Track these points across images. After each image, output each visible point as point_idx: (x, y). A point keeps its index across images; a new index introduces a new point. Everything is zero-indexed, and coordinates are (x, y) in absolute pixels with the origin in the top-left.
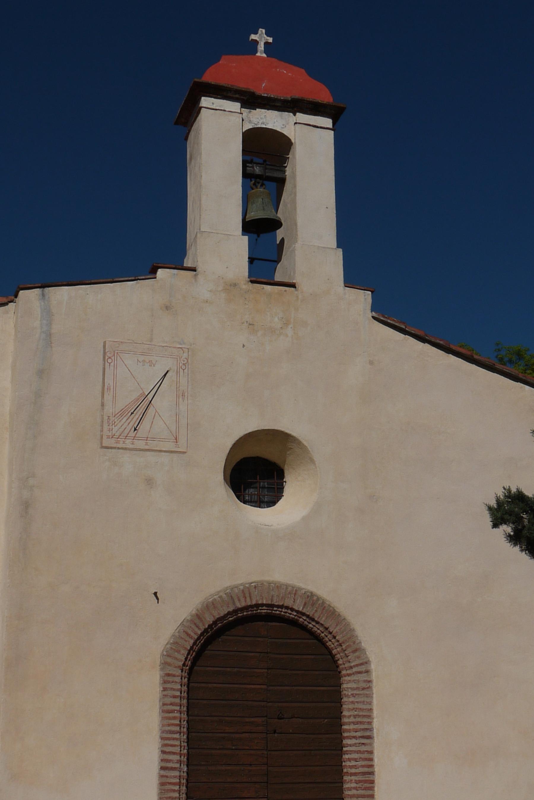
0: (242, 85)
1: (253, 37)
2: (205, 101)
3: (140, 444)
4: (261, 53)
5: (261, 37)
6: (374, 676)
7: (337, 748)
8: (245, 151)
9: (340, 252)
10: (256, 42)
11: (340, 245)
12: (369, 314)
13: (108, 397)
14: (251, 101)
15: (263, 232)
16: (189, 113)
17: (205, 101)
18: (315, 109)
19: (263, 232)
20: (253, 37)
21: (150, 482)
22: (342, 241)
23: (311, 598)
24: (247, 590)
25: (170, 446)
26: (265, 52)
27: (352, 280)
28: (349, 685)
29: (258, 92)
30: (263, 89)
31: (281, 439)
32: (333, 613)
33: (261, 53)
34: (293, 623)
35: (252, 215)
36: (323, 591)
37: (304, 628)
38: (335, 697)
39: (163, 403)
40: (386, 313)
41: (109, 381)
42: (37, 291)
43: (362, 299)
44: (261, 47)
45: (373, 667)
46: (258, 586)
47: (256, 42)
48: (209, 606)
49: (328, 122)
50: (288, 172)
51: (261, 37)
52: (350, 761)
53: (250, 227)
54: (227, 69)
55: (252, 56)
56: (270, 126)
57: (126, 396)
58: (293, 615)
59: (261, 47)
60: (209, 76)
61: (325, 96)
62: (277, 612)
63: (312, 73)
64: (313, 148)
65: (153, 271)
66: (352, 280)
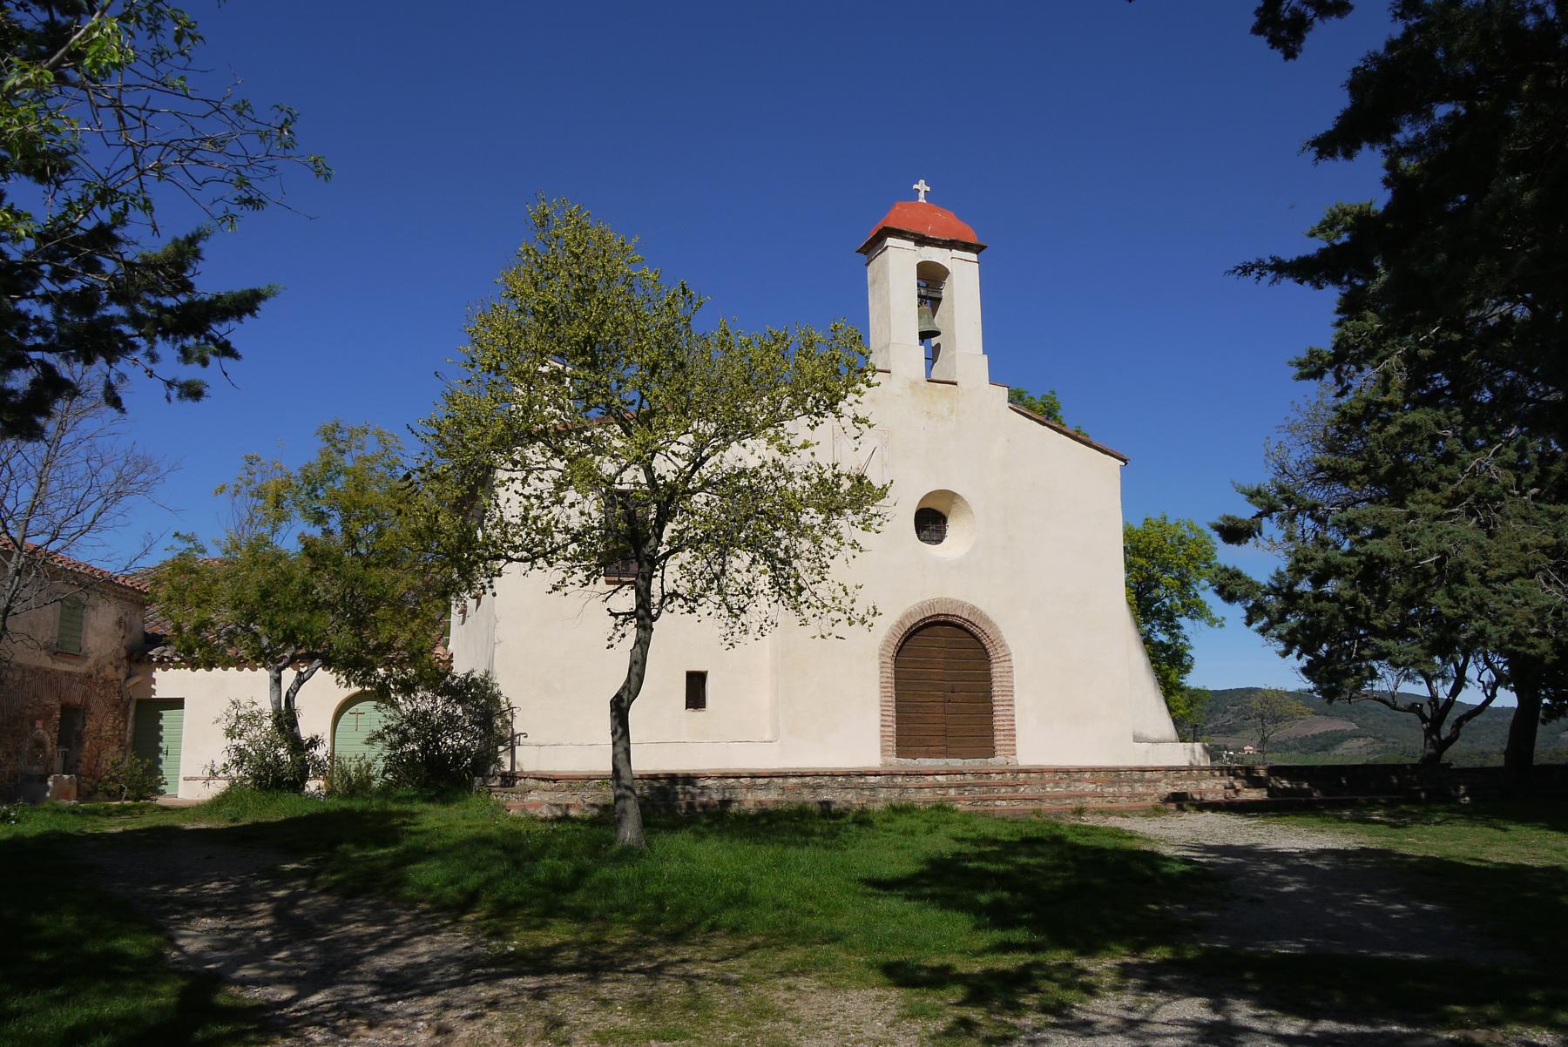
0: (915, 230)
4: (922, 199)
6: (1014, 664)
7: (990, 713)
14: (921, 241)
16: (874, 245)
17: (890, 241)
22: (987, 350)
23: (973, 610)
24: (931, 605)
27: (994, 380)
28: (997, 670)
31: (950, 496)
32: (987, 620)
33: (922, 199)
34: (960, 627)
36: (982, 605)
37: (967, 630)
38: (988, 678)
45: (1013, 657)
46: (939, 601)
48: (908, 615)
49: (973, 256)
50: (944, 294)
52: (999, 721)
58: (960, 622)
62: (954, 619)
64: (963, 272)
66: (996, 377)
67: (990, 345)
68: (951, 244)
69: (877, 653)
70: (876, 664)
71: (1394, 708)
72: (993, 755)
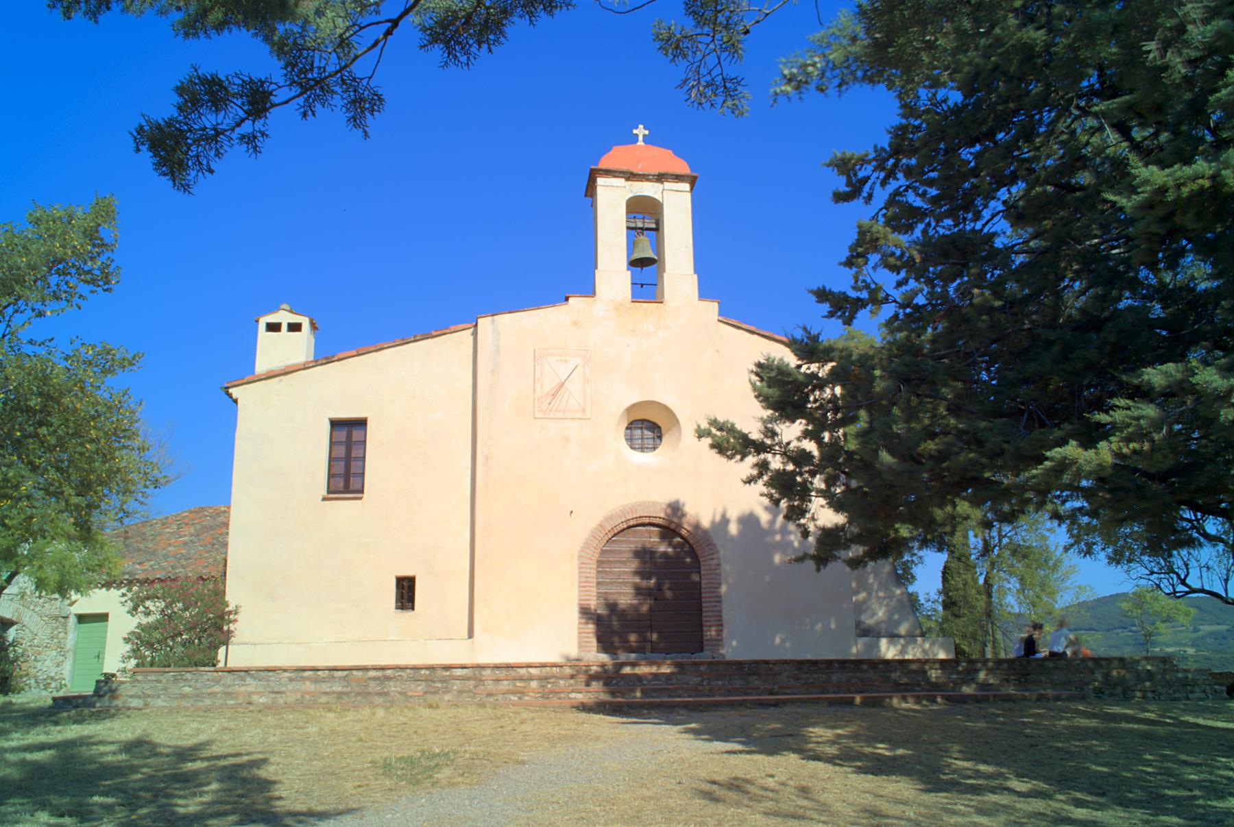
0: (624, 168)
1: (635, 131)
2: (600, 181)
3: (560, 415)
4: (641, 143)
5: (641, 131)
8: (628, 213)
9: (695, 277)
10: (637, 135)
11: (695, 272)
12: (716, 317)
13: (538, 386)
14: (631, 176)
15: (646, 269)
16: (590, 190)
18: (678, 178)
19: (646, 269)
20: (635, 131)
21: (567, 439)
22: (697, 270)
25: (580, 415)
26: (644, 141)
27: (704, 294)
29: (635, 172)
30: (638, 170)
35: (637, 255)
39: (573, 386)
40: (729, 315)
41: (538, 375)
42: (489, 318)
43: (712, 308)
44: (641, 138)
47: (637, 135)
48: (609, 518)
51: (641, 131)
53: (637, 264)
54: (616, 157)
55: (631, 146)
56: (646, 194)
57: (549, 385)
59: (641, 138)
60: (604, 163)
61: (683, 168)
63: (678, 154)
64: (677, 205)
65: (567, 299)
66: (704, 294)
67: (700, 266)
68: (660, 178)
69: (576, 554)
70: (576, 563)
71: (1228, 603)
72: (702, 650)
